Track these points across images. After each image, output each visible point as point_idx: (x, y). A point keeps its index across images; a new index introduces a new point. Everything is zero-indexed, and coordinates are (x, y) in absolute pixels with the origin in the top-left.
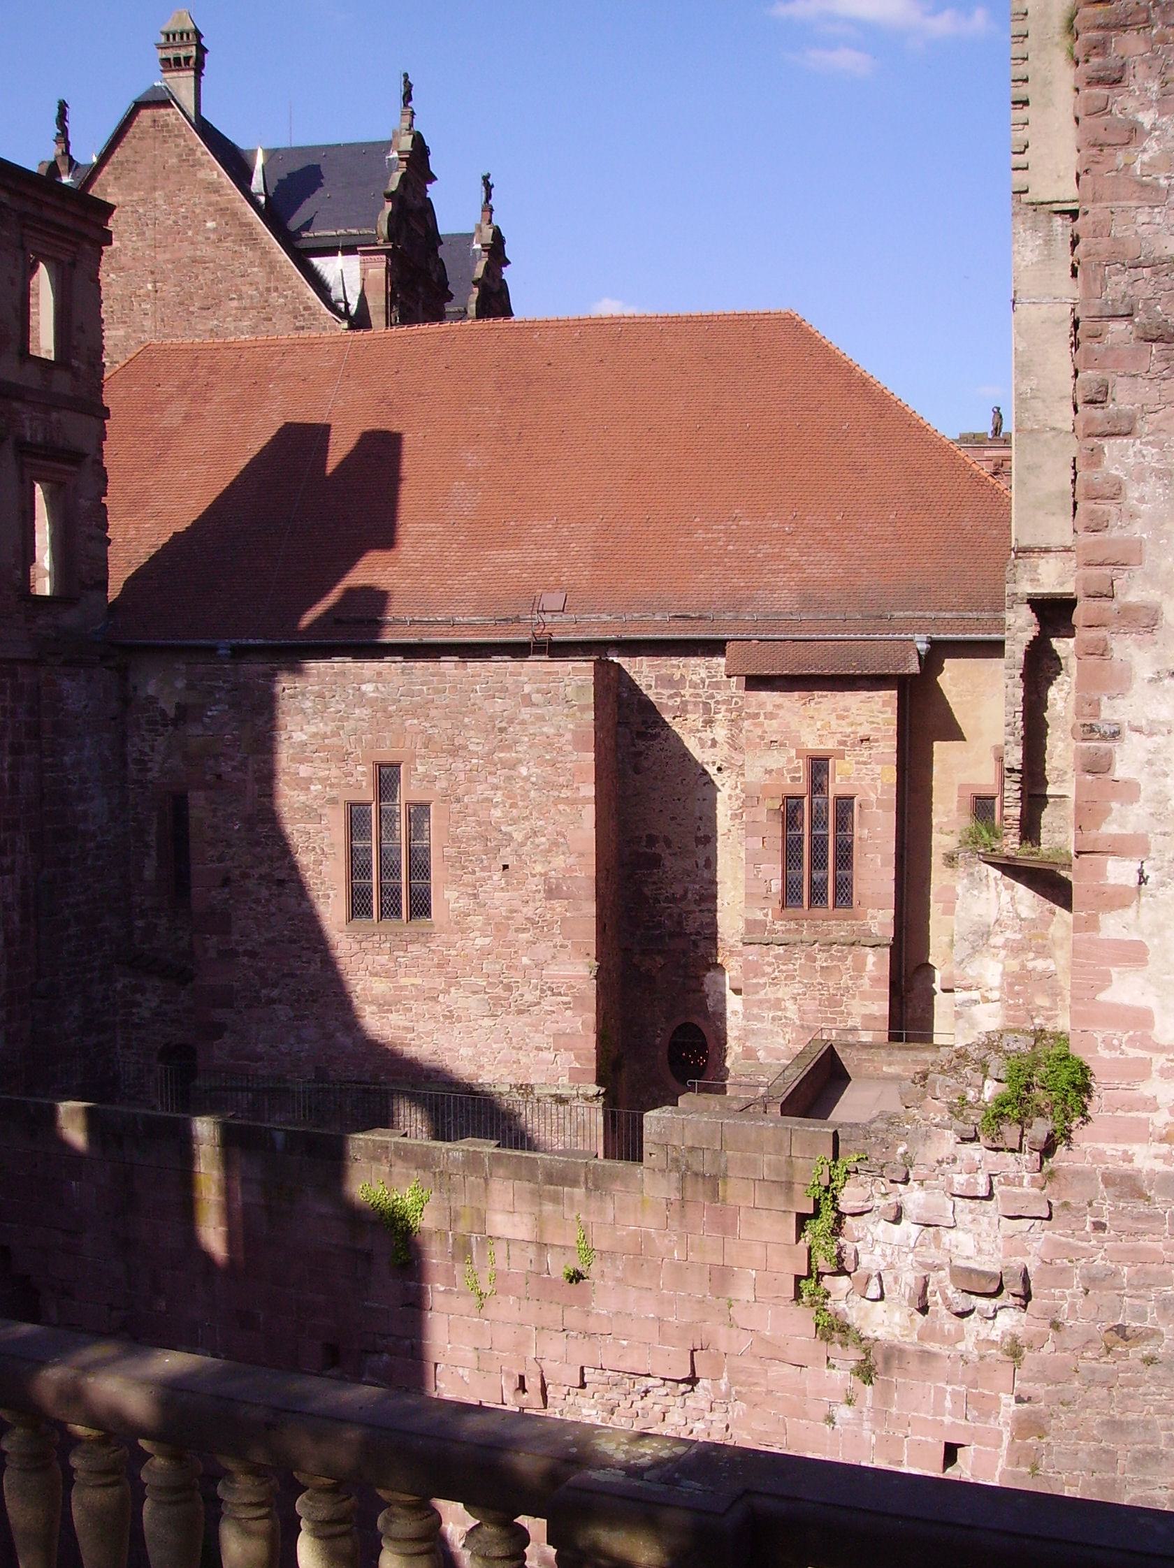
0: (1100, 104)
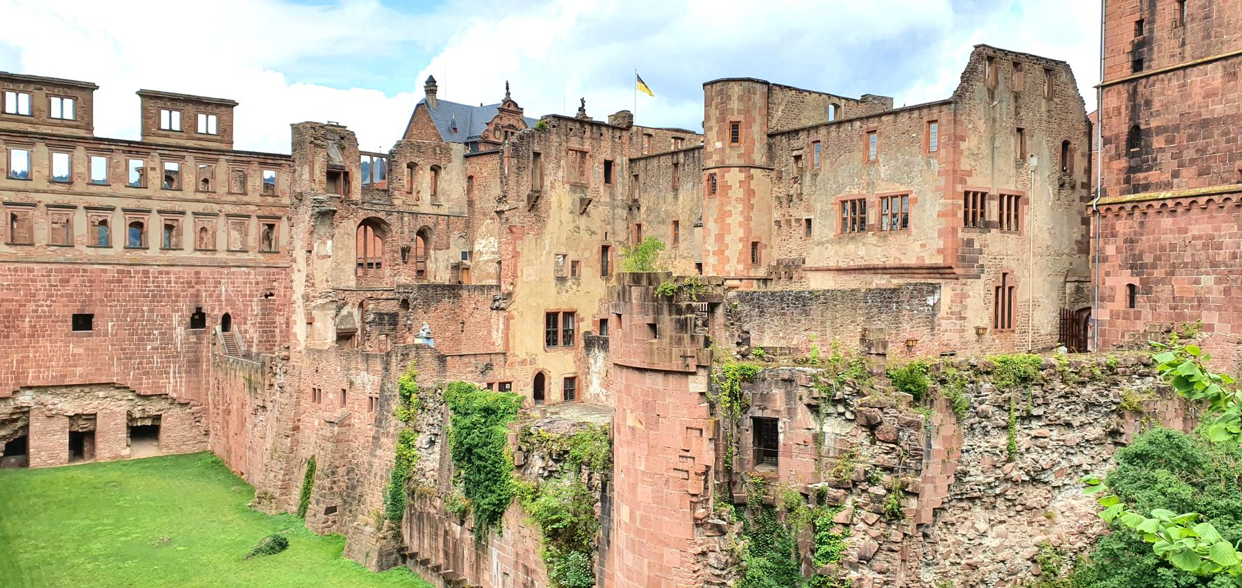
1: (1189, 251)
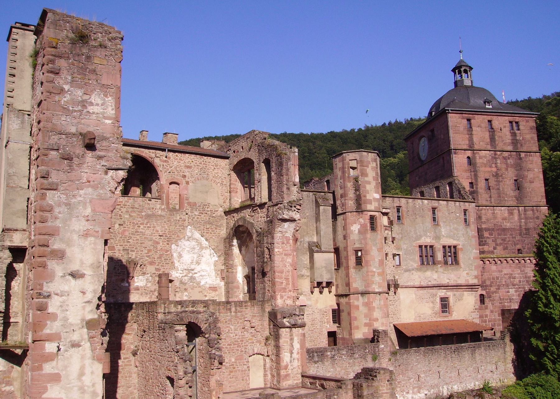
0: (51, 79)
1: (504, 281)
